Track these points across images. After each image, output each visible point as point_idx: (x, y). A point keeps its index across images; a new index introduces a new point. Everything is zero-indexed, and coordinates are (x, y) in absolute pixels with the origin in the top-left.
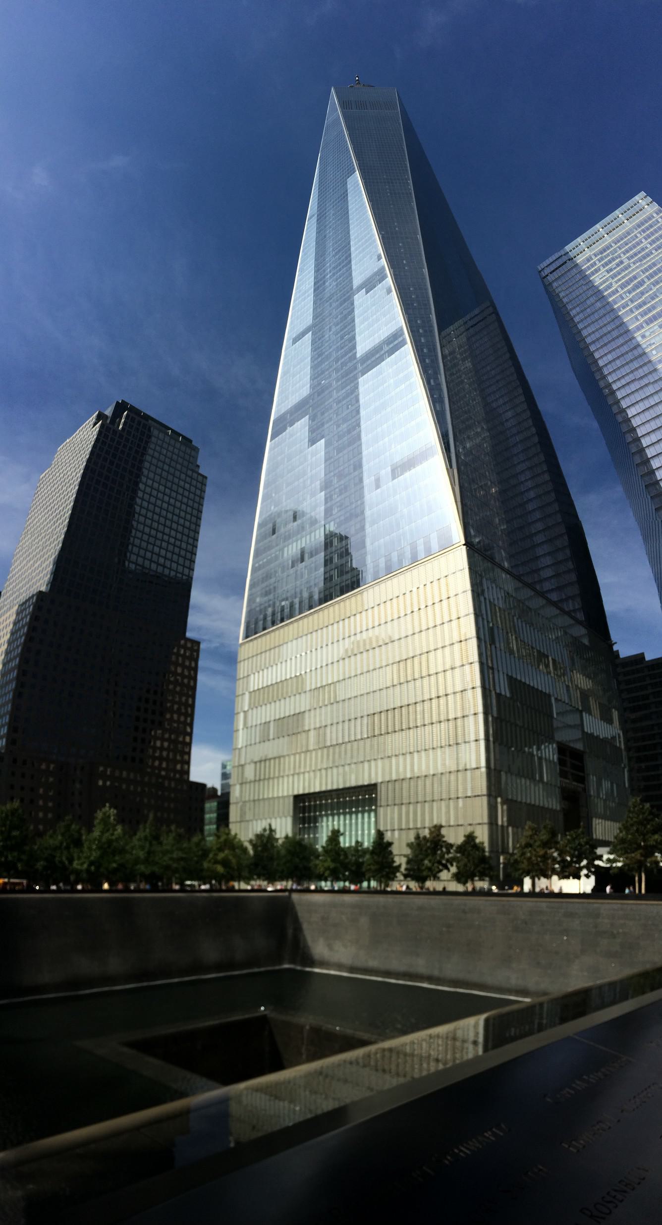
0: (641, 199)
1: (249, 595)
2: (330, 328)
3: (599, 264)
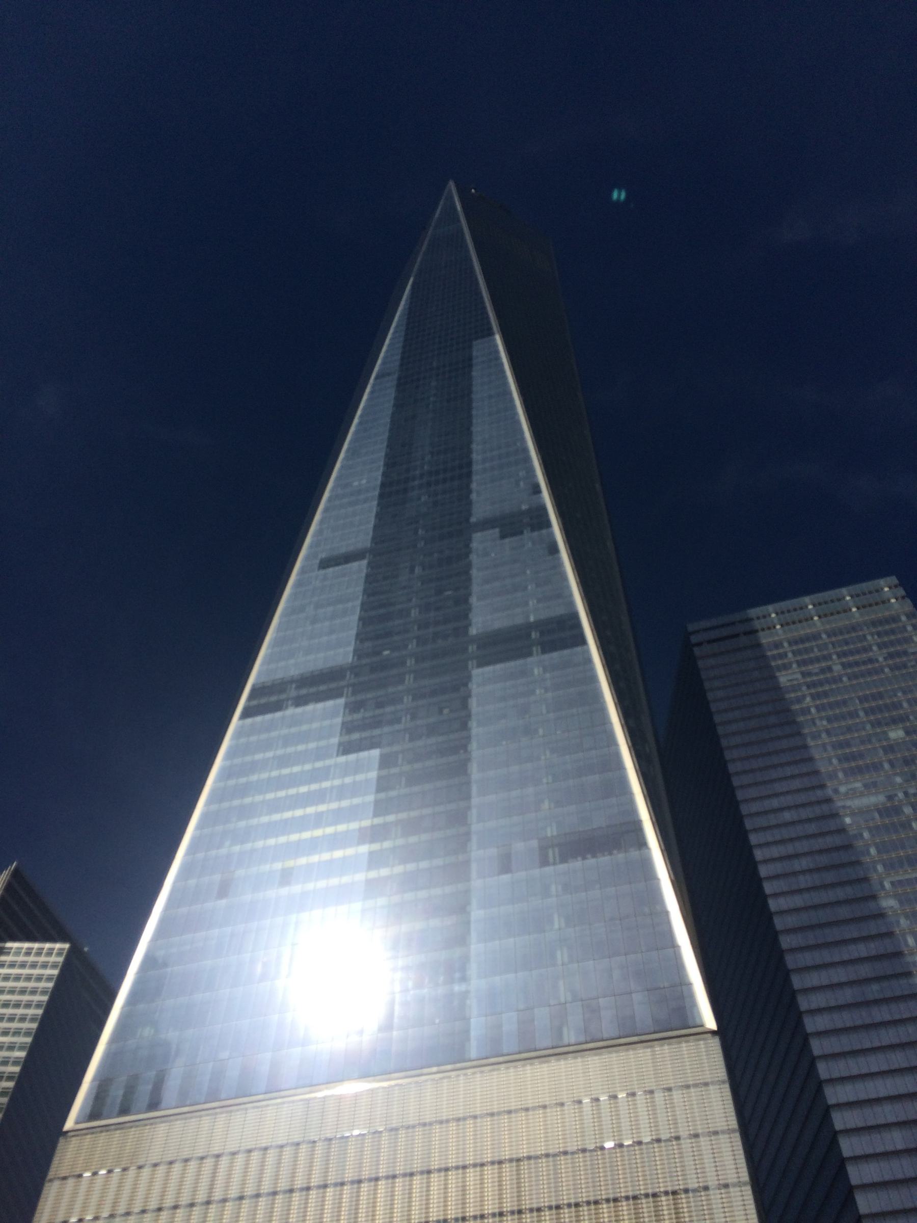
0: (886, 586)
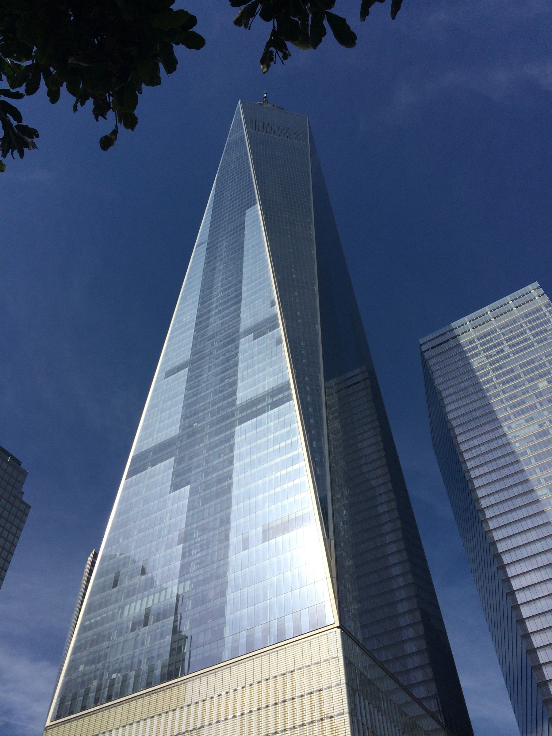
0: (533, 290)
1: (71, 661)
2: (210, 367)
3: (480, 348)
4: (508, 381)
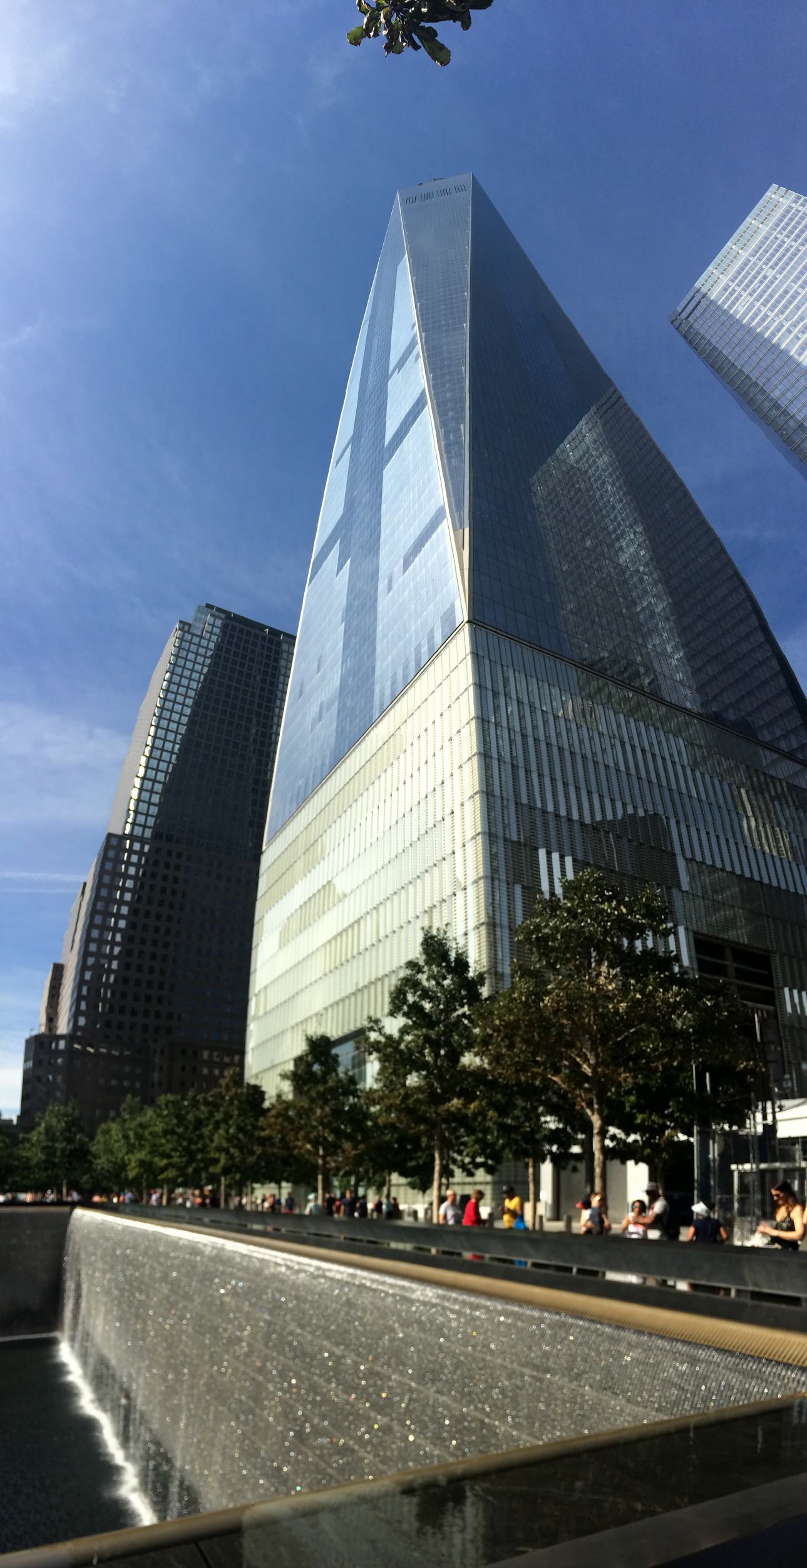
3: (739, 290)
4: (786, 307)
